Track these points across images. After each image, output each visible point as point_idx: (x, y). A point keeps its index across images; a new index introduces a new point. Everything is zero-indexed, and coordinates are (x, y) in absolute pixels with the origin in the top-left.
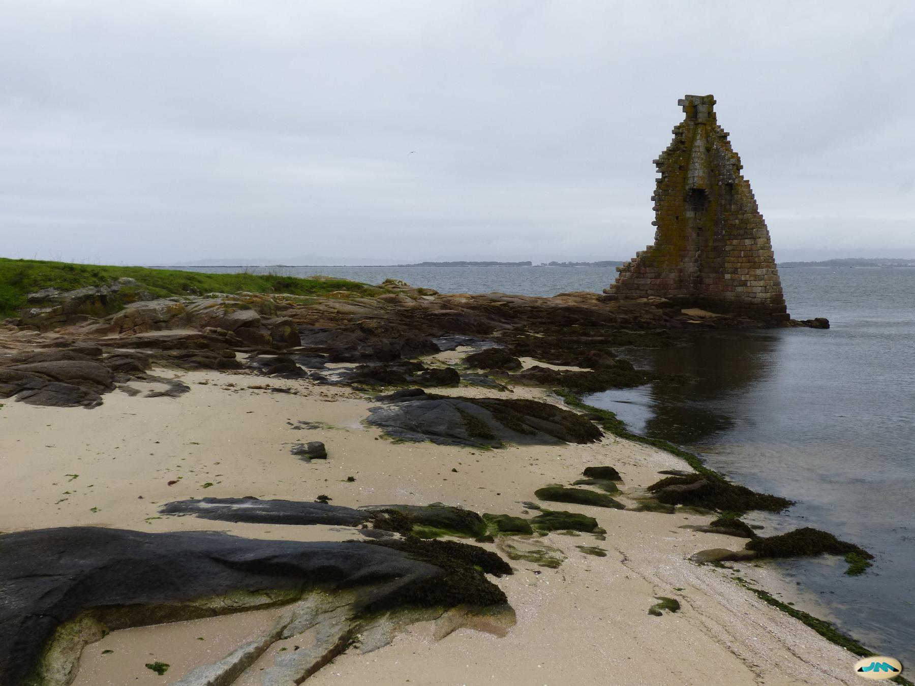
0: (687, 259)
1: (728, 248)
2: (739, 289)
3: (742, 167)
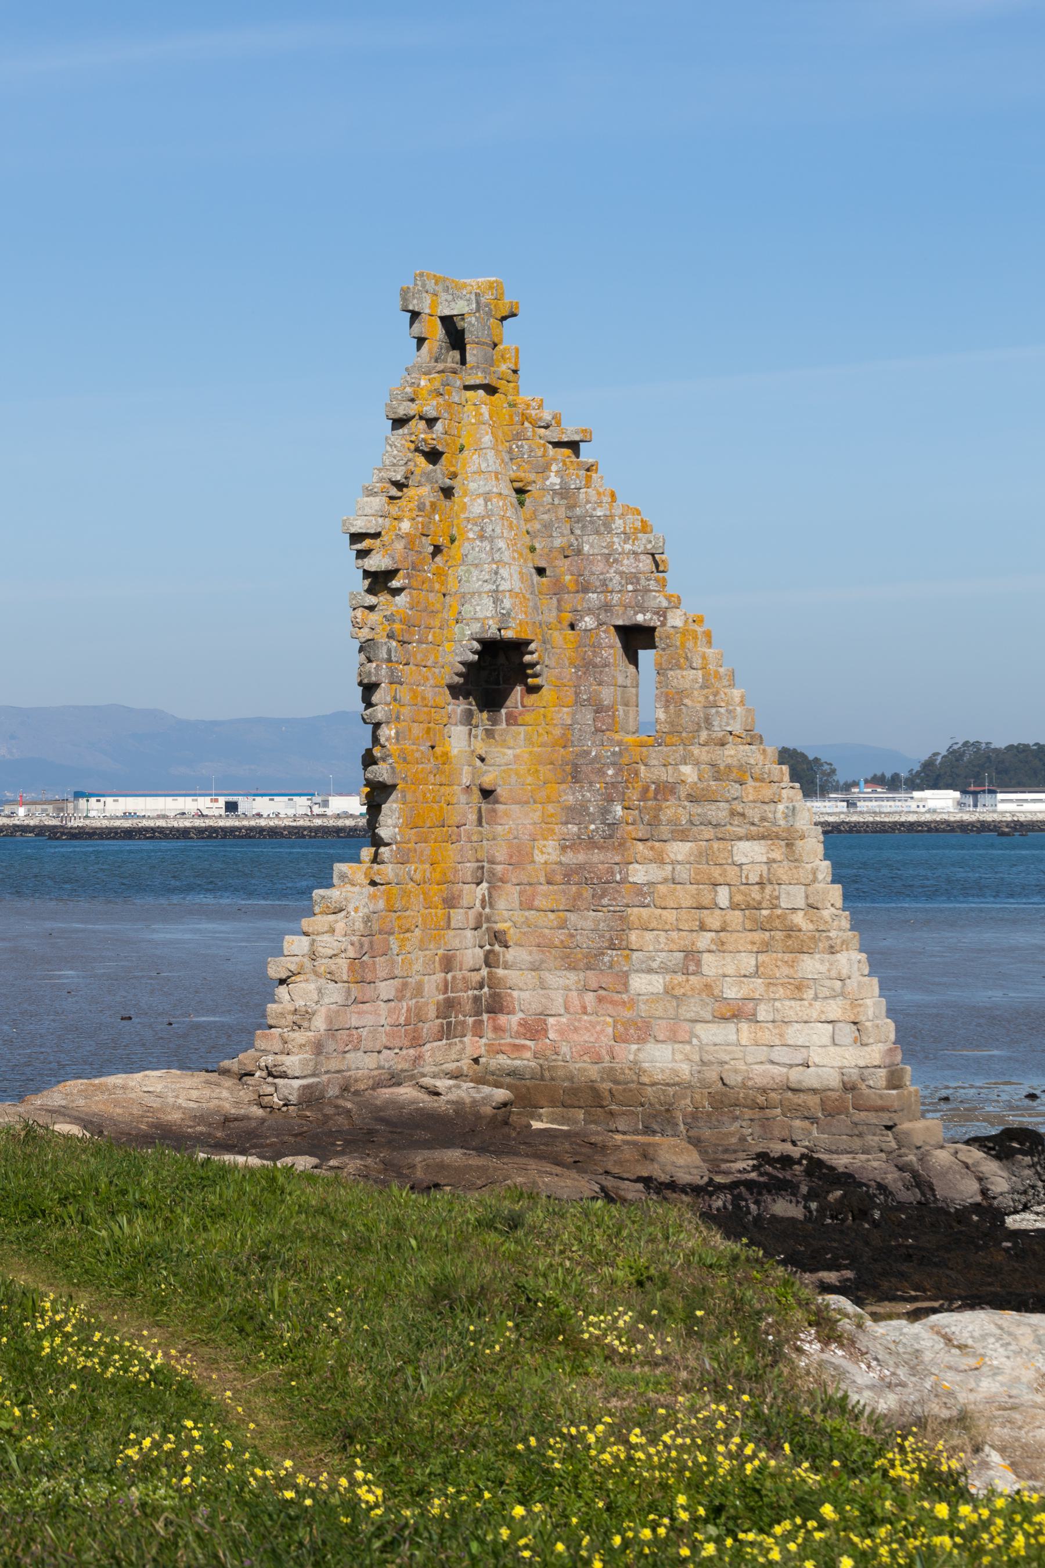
0: (458, 916)
2: (712, 1034)
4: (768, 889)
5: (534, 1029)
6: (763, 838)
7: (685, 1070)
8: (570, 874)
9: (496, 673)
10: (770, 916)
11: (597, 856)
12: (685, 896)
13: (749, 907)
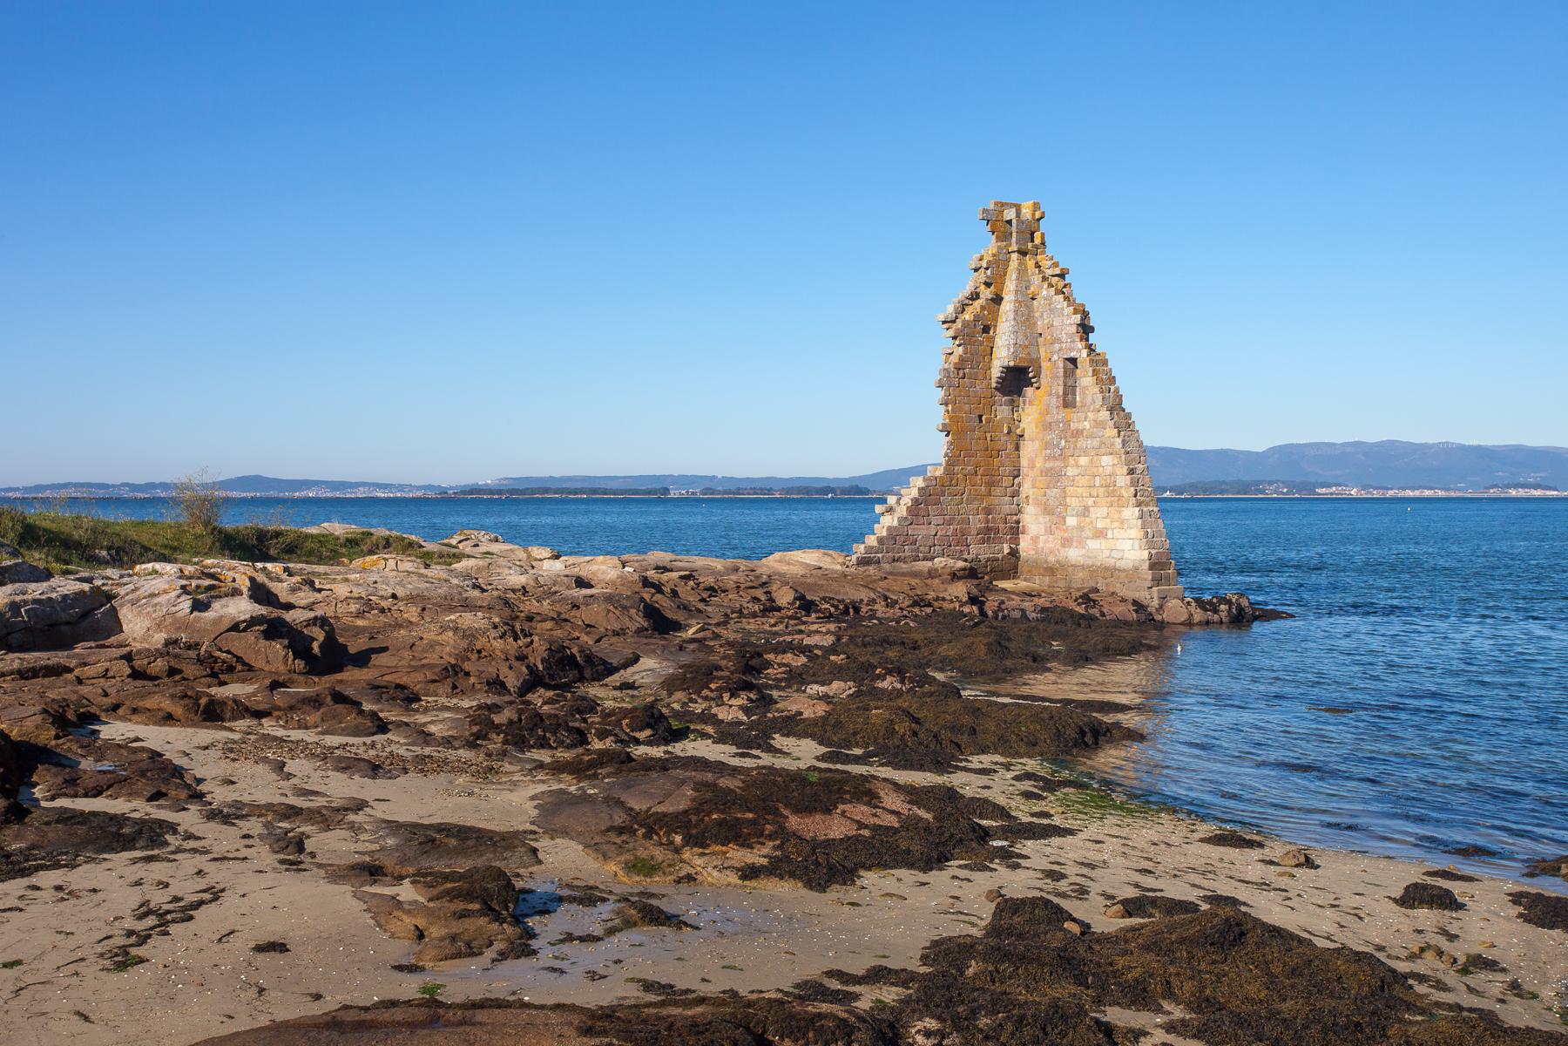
0: (997, 491)
1: (1070, 472)
2: (1093, 544)
3: (1092, 329)
5: (1035, 539)
7: (1082, 561)
8: (1046, 472)
9: (1017, 380)
11: (1057, 464)
12: (1084, 481)
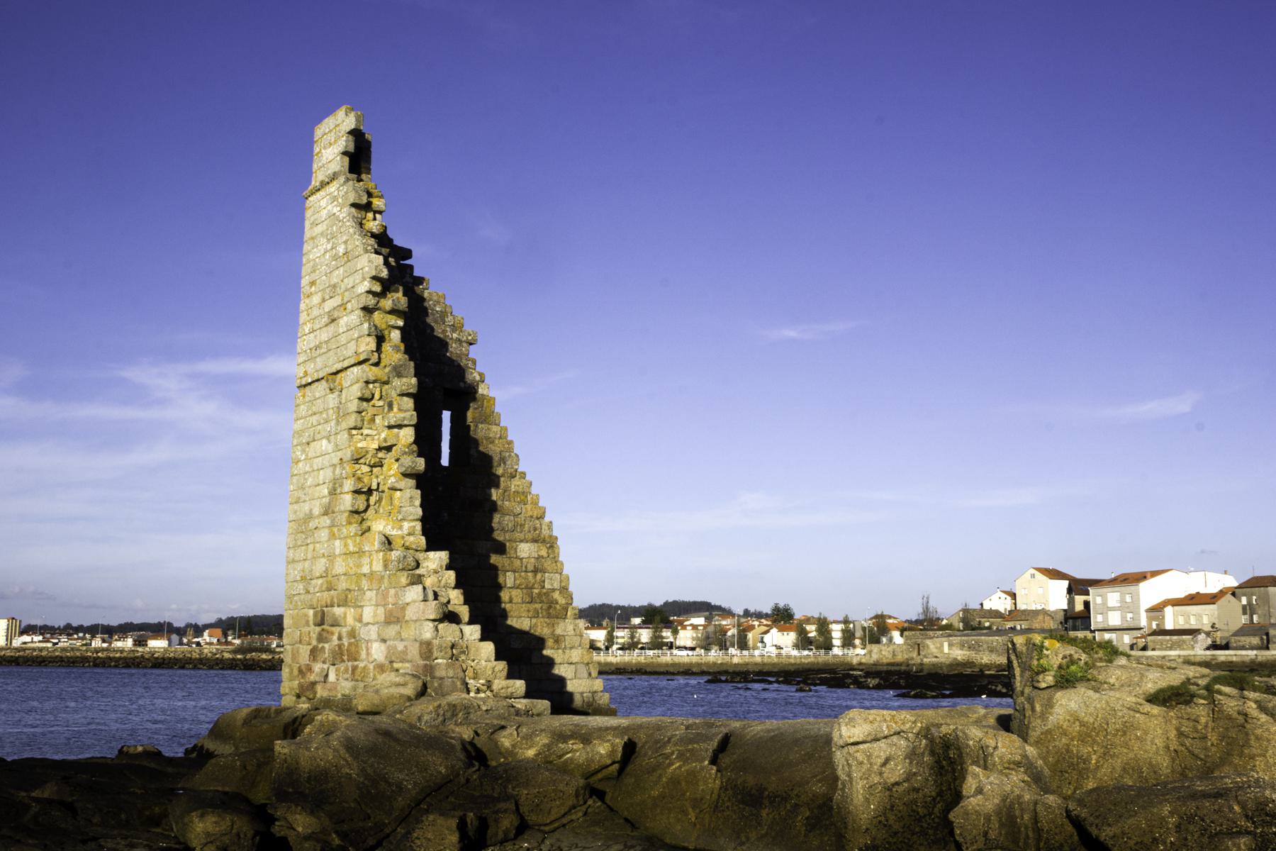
4: (539, 576)
6: (535, 541)
10: (539, 595)
13: (527, 587)
